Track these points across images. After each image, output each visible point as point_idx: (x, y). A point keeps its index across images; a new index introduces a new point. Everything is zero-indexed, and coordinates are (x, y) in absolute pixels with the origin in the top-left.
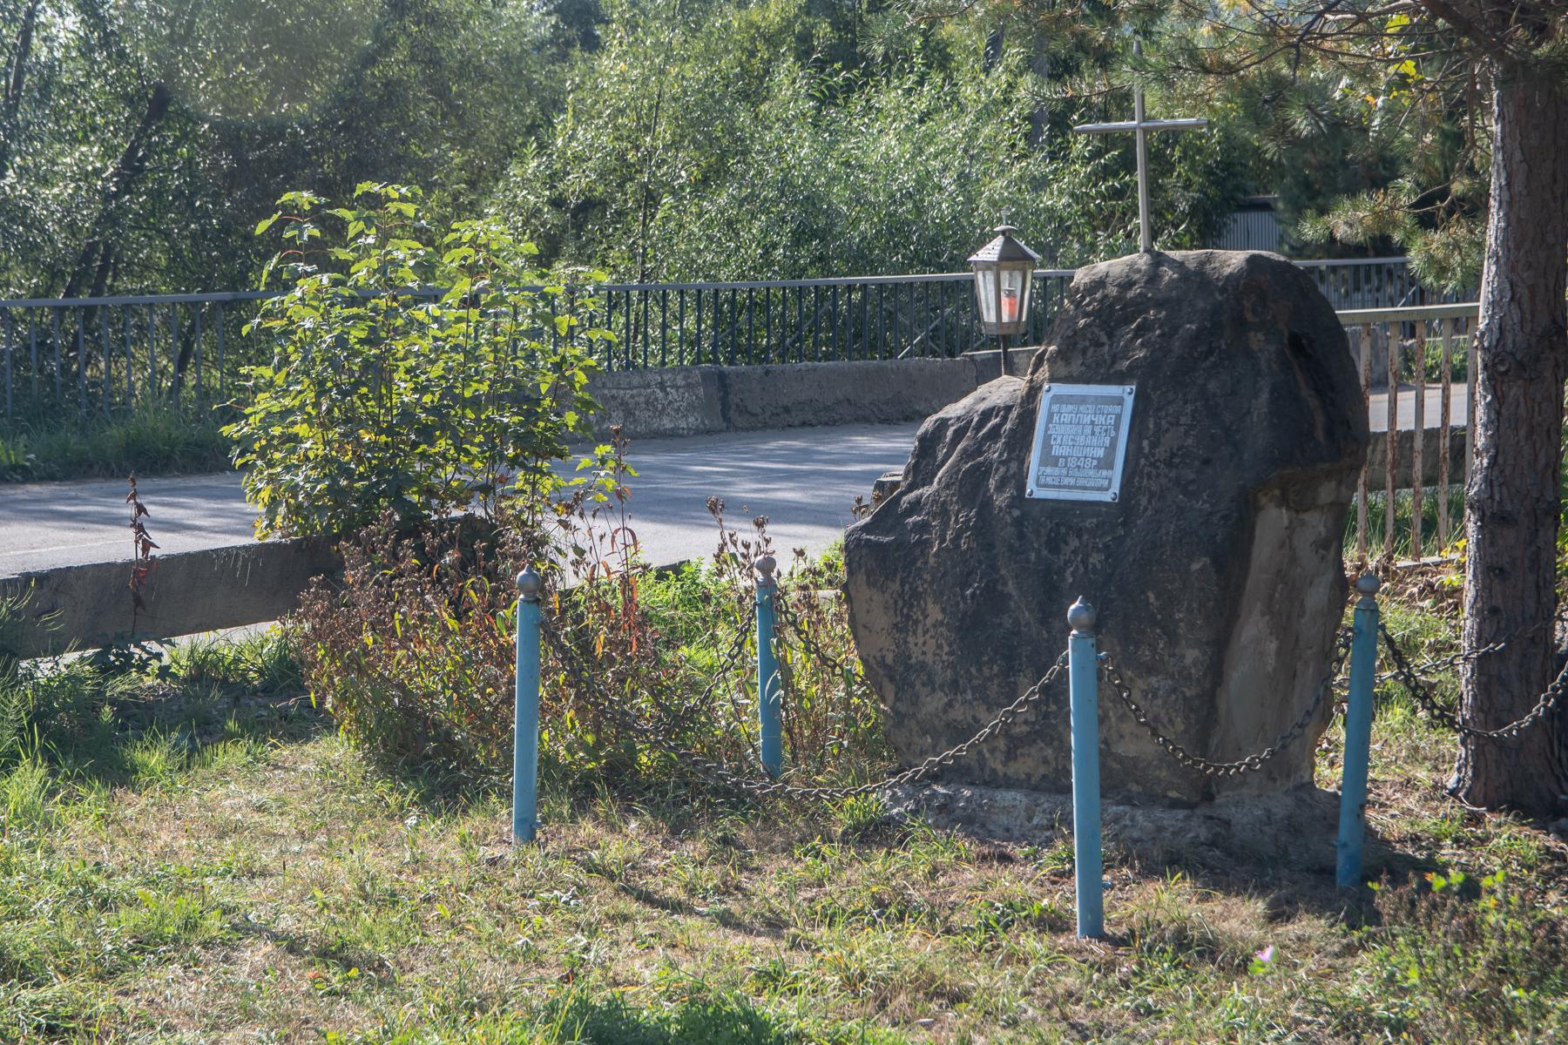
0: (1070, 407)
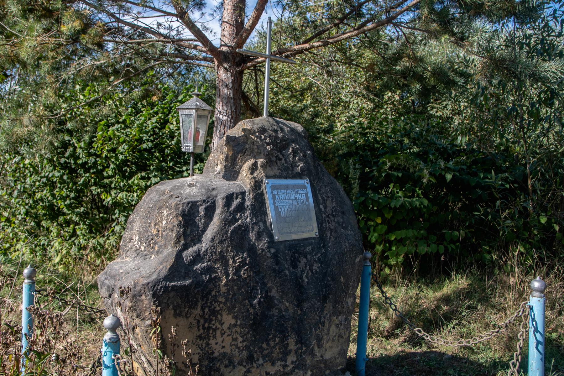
0: (282, 191)
